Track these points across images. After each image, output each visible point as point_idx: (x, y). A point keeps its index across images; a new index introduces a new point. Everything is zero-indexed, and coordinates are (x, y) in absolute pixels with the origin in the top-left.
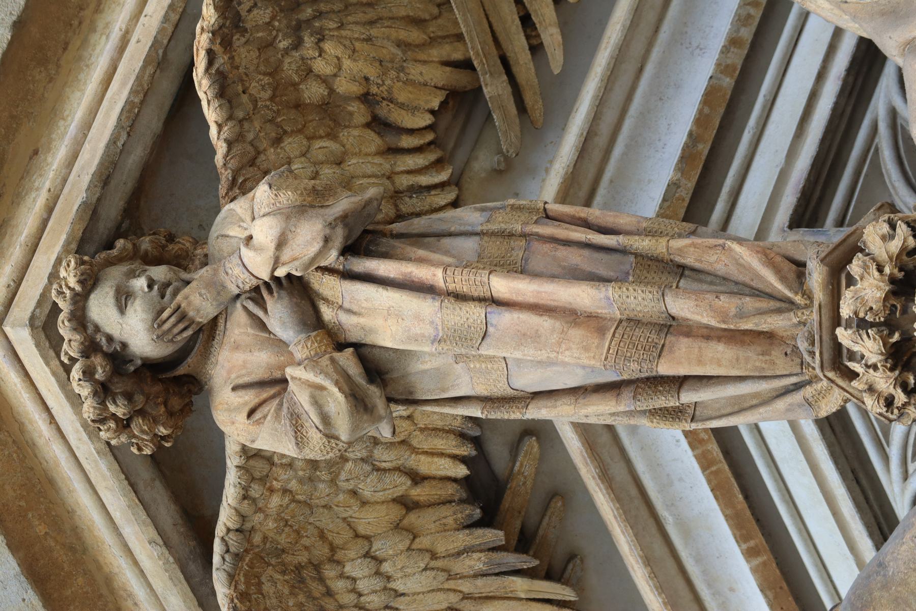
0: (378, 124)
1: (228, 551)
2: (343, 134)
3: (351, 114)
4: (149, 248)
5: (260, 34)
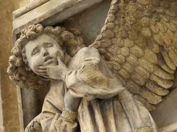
0: (160, 56)
1: (33, 126)
2: (147, 51)
3: (153, 47)
4: (63, 37)
5: (140, 6)
